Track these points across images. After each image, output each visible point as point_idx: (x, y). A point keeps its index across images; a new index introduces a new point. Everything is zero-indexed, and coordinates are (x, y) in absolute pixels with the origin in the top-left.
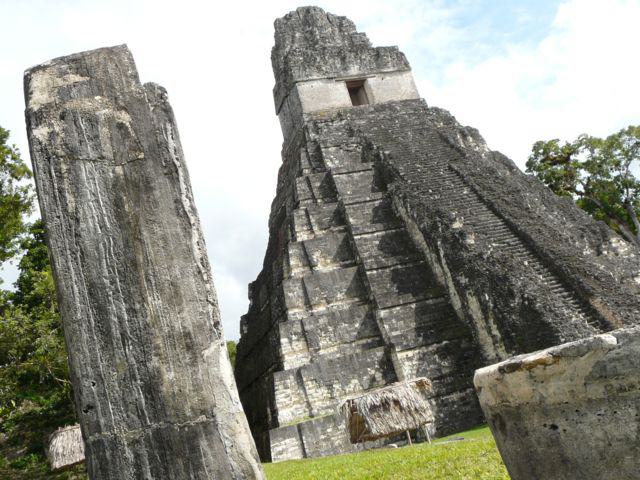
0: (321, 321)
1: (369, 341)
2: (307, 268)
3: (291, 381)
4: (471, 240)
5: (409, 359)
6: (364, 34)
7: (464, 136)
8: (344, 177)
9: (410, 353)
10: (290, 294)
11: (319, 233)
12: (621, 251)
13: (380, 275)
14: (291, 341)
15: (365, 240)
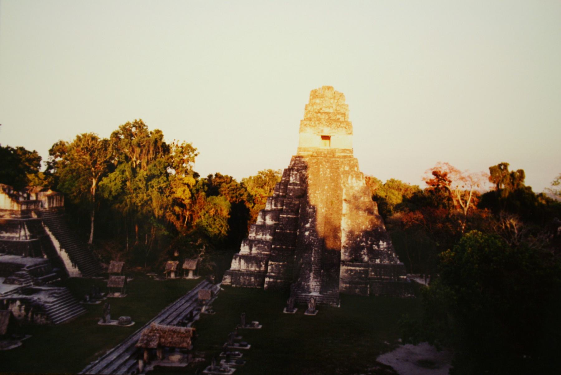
0: (256, 242)
1: (268, 253)
2: (263, 221)
3: (238, 259)
4: (307, 233)
5: (271, 265)
6: (348, 106)
7: (352, 176)
8: (291, 187)
9: (273, 263)
10: (252, 230)
11: (274, 207)
12: (381, 247)
13: (280, 232)
14: (244, 246)
15: (283, 217)
